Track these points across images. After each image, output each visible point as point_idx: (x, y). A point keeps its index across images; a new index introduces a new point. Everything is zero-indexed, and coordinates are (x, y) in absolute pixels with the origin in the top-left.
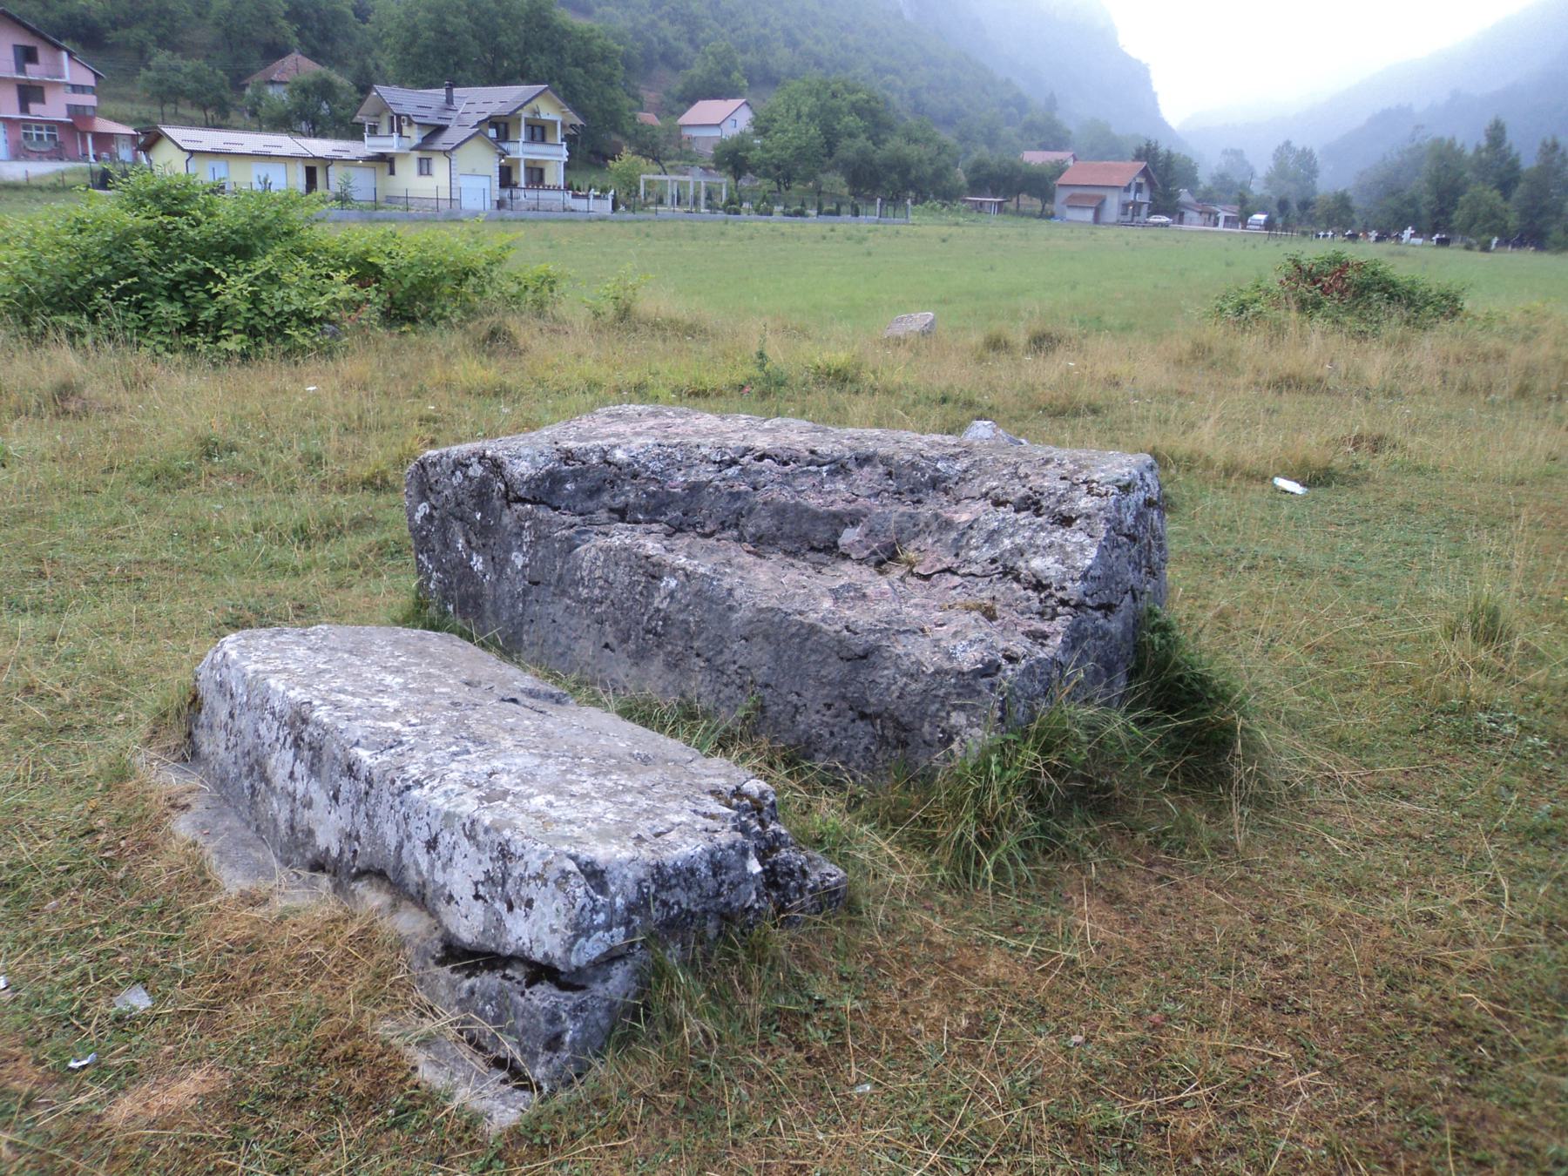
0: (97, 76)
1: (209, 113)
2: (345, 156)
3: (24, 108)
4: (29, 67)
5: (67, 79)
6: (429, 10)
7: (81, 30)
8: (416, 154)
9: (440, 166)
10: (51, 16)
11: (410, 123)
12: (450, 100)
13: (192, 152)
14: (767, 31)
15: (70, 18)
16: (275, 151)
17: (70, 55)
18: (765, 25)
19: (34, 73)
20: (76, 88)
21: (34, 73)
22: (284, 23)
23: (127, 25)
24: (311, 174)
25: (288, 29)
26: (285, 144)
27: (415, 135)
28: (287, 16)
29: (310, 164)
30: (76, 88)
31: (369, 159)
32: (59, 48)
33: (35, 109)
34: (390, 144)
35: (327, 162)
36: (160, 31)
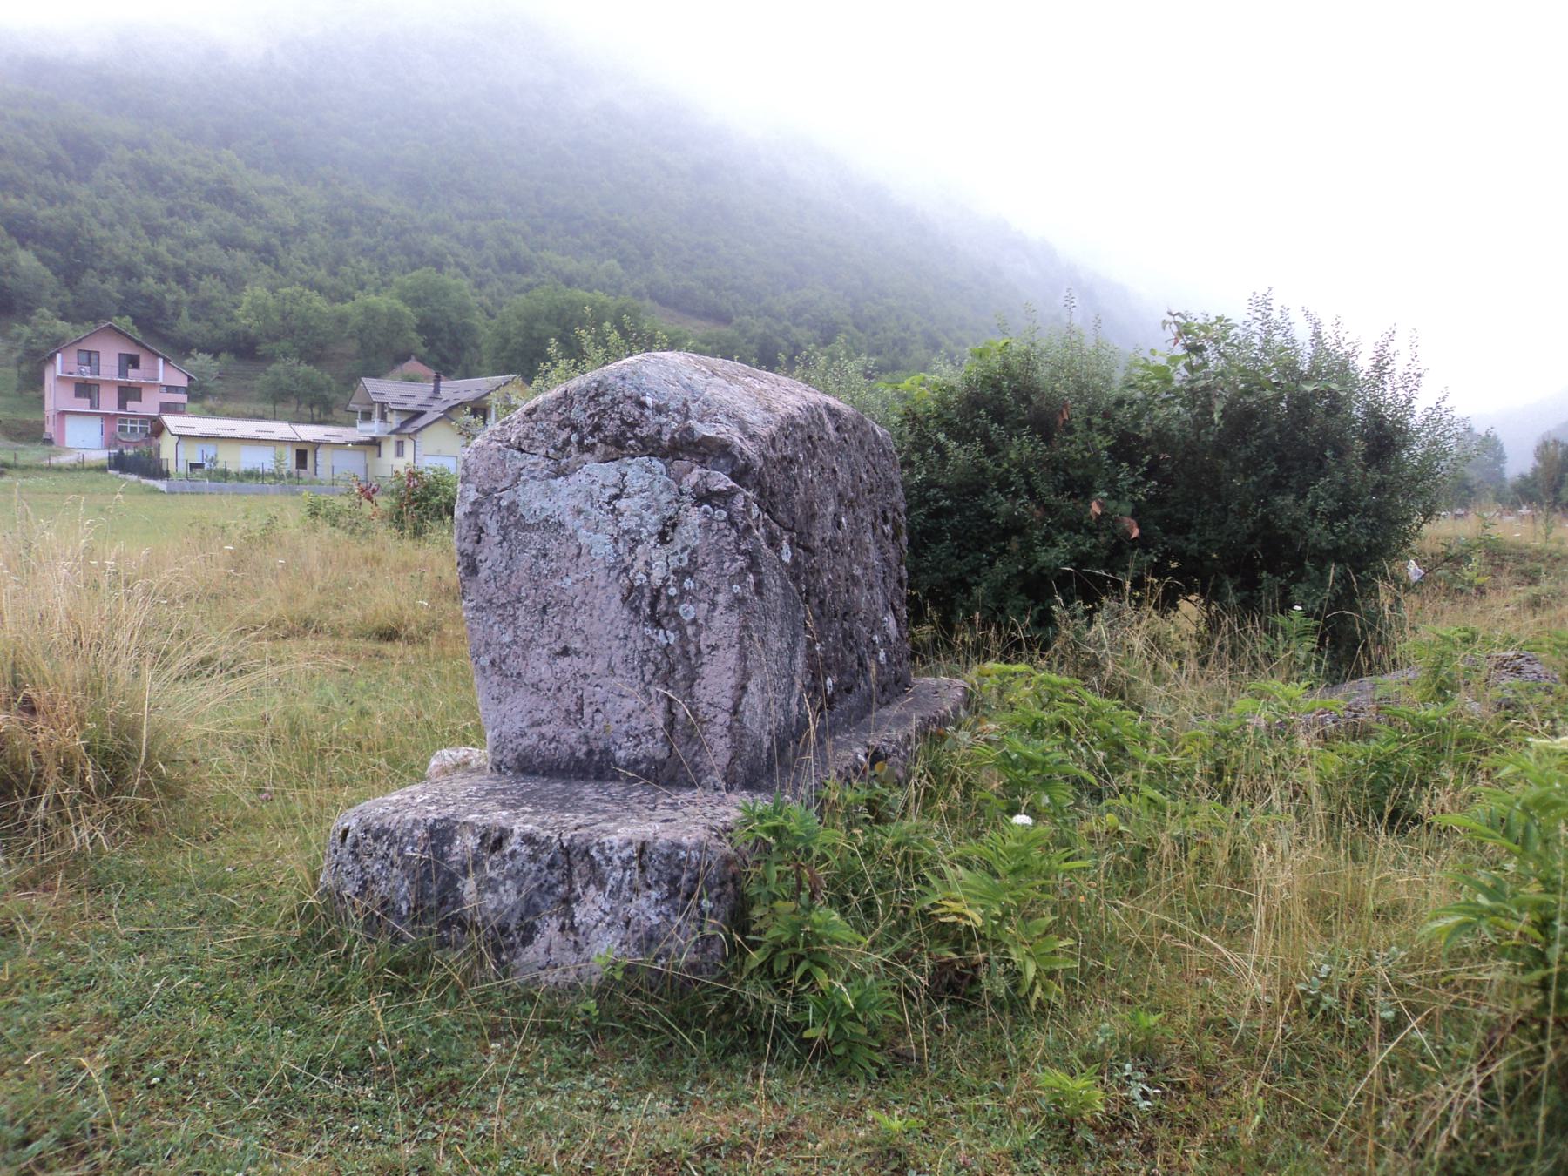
0: (190, 379)
1: (316, 411)
2: (333, 440)
3: (122, 405)
4: (131, 372)
5: (161, 381)
6: (519, 317)
7: (242, 345)
8: (394, 437)
9: (408, 447)
10: (217, 333)
11: (391, 410)
12: (437, 390)
13: (180, 436)
14: (906, 335)
15: (234, 334)
16: (262, 436)
17: (166, 361)
18: (906, 328)
19: (134, 376)
20: (170, 389)
21: (134, 376)
22: (413, 335)
23: (276, 339)
24: (301, 458)
25: (416, 340)
26: (281, 430)
27: (394, 421)
28: (421, 329)
29: (302, 447)
30: (170, 389)
31: (361, 443)
32: (158, 356)
33: (132, 406)
34: (373, 429)
35: (317, 445)
36: (303, 344)
